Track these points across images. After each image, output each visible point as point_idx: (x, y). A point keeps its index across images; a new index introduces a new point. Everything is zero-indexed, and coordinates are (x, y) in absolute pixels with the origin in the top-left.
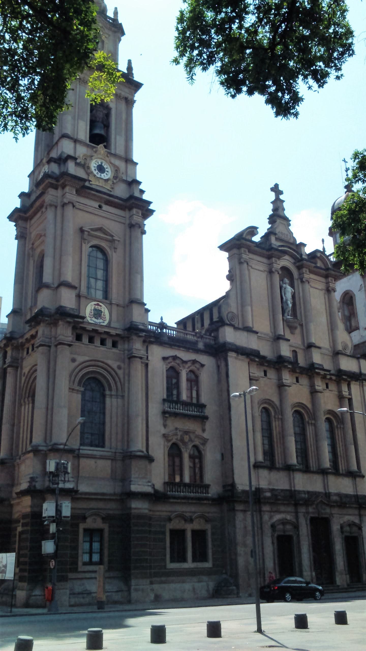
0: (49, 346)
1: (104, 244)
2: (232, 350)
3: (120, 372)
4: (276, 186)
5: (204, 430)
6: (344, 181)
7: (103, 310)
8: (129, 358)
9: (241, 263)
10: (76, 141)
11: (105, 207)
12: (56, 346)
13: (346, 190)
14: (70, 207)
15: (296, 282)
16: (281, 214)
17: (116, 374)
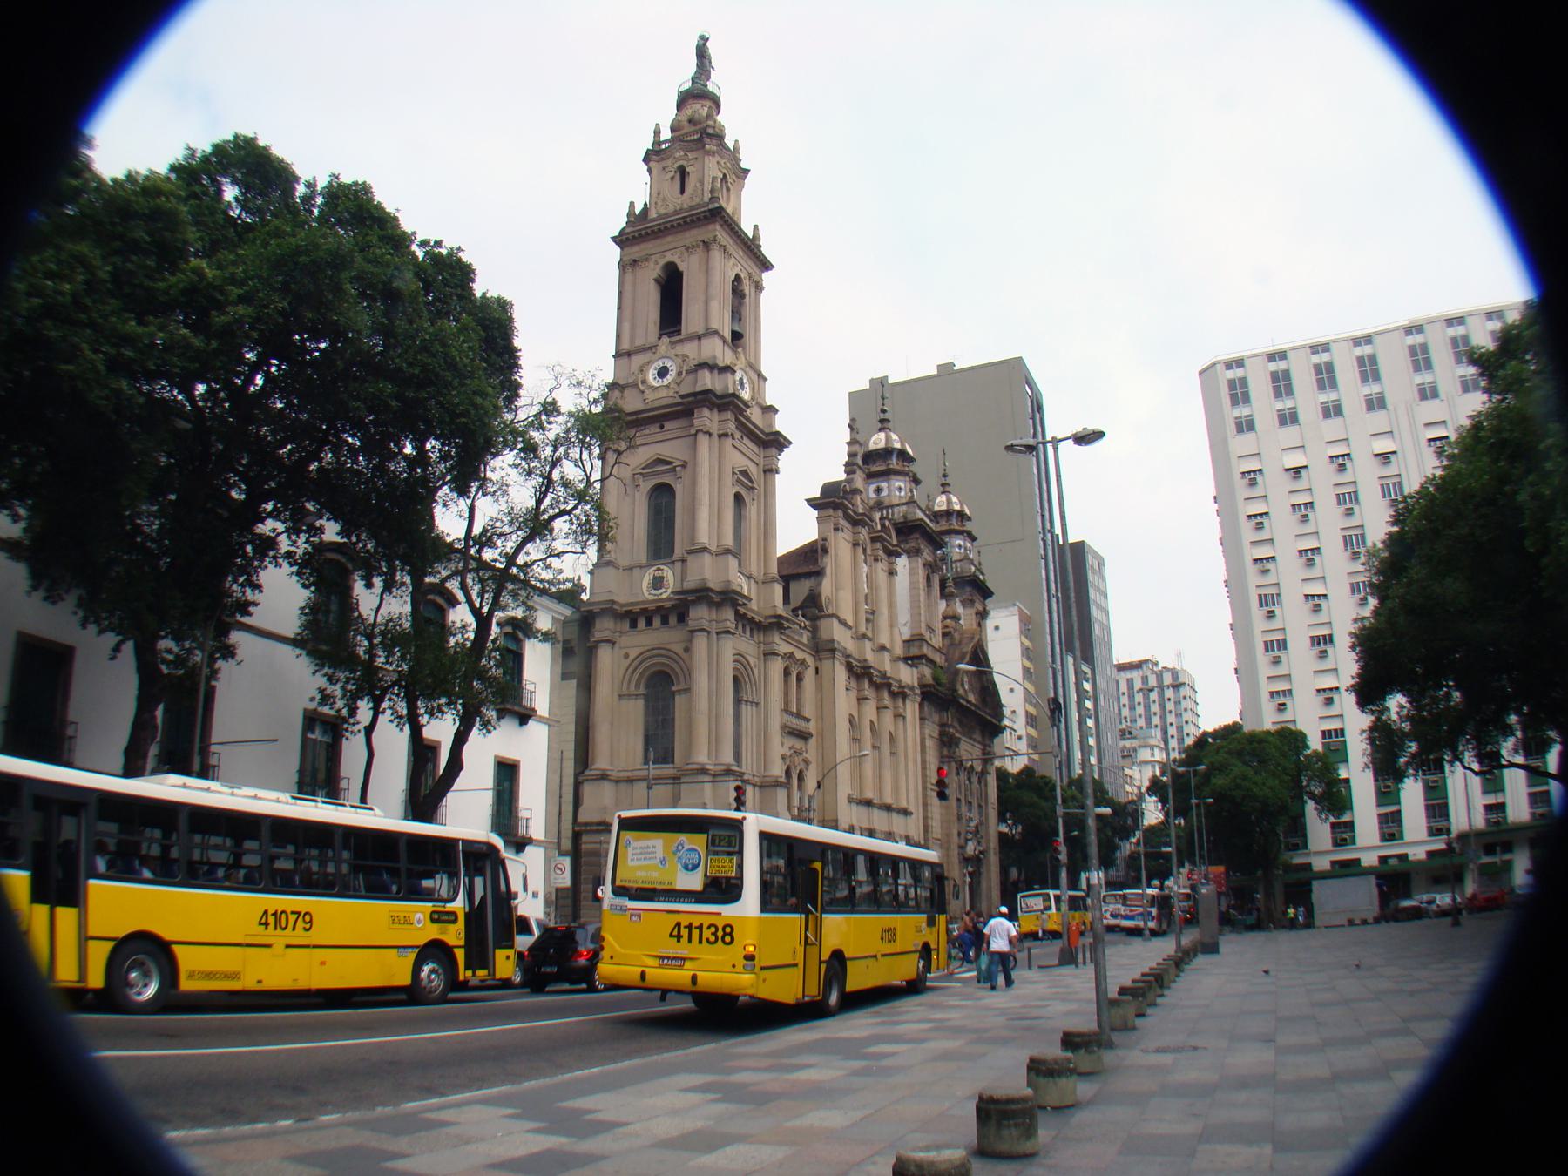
1: (743, 492)
8: (765, 655)
9: (836, 529)
11: (746, 441)
14: (729, 441)
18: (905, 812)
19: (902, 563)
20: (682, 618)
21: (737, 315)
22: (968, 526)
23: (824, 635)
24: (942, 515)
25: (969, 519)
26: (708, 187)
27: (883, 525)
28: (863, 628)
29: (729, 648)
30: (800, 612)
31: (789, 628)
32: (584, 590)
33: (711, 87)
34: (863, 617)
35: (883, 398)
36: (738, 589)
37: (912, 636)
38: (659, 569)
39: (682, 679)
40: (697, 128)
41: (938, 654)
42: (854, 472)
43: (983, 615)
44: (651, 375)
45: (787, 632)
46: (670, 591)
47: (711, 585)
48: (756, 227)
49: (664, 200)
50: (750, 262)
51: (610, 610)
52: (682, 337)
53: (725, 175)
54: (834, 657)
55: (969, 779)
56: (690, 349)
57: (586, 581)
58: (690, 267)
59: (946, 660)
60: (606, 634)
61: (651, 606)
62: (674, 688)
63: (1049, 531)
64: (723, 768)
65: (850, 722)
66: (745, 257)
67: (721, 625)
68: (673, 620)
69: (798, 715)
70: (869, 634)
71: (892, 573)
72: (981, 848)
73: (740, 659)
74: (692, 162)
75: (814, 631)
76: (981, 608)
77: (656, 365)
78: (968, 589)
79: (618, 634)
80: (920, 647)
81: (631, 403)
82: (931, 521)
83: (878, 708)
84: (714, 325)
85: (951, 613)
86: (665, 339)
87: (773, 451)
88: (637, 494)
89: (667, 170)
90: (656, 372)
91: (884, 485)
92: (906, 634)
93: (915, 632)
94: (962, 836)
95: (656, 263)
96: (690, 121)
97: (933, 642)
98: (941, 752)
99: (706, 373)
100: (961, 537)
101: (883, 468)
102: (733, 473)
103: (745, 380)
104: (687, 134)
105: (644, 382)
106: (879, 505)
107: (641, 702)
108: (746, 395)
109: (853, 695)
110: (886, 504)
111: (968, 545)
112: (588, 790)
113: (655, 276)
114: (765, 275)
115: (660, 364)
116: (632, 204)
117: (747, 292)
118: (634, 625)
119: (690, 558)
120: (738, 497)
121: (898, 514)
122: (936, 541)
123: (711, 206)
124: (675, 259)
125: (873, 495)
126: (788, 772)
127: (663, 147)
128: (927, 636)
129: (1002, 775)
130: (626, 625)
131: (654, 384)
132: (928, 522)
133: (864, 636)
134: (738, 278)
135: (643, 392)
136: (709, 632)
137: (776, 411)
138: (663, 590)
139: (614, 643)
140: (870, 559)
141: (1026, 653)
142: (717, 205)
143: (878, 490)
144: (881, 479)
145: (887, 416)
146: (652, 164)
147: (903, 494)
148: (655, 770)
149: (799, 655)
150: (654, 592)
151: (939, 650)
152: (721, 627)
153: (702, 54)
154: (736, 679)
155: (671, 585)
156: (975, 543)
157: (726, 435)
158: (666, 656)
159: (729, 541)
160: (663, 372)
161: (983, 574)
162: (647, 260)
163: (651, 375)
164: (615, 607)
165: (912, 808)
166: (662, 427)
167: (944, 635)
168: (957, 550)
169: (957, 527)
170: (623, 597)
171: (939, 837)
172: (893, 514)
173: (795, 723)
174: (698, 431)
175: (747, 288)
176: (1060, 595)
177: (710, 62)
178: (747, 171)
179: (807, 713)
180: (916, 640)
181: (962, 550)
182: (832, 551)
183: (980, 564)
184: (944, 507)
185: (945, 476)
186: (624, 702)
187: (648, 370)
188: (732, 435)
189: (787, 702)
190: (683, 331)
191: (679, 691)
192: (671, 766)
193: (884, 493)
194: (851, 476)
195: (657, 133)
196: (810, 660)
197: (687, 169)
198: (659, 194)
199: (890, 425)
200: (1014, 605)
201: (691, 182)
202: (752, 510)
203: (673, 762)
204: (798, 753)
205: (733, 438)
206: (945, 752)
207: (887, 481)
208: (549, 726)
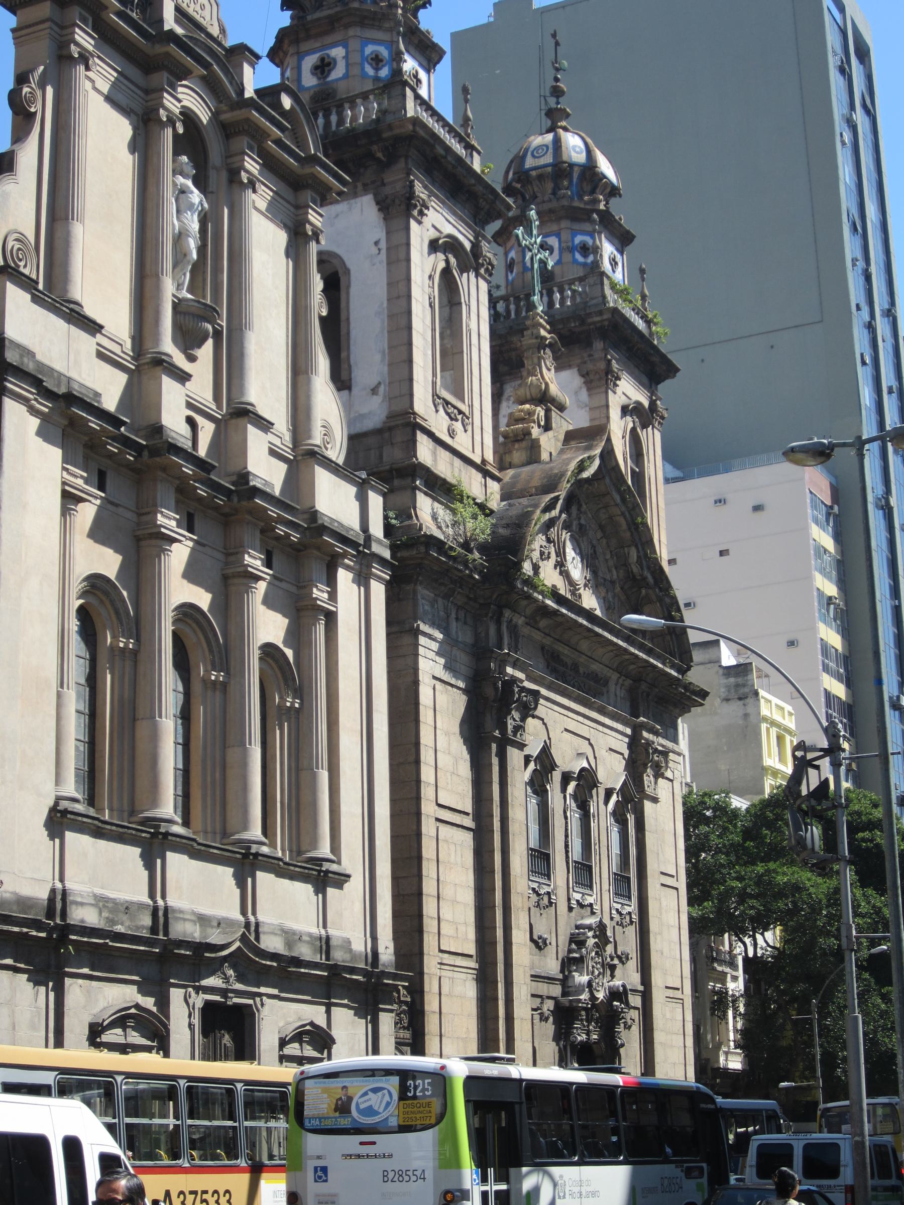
15: (212, 174)
25: (613, 192)
37: (391, 417)
41: (477, 477)
55: (583, 806)
70: (179, 359)
91: (338, 52)
97: (462, 443)
125: (309, 80)
128: (439, 423)
143: (323, 67)
144: (329, 39)
151: (482, 469)
161: (648, 322)
168: (579, 257)
185: (557, 92)
193: (338, 73)
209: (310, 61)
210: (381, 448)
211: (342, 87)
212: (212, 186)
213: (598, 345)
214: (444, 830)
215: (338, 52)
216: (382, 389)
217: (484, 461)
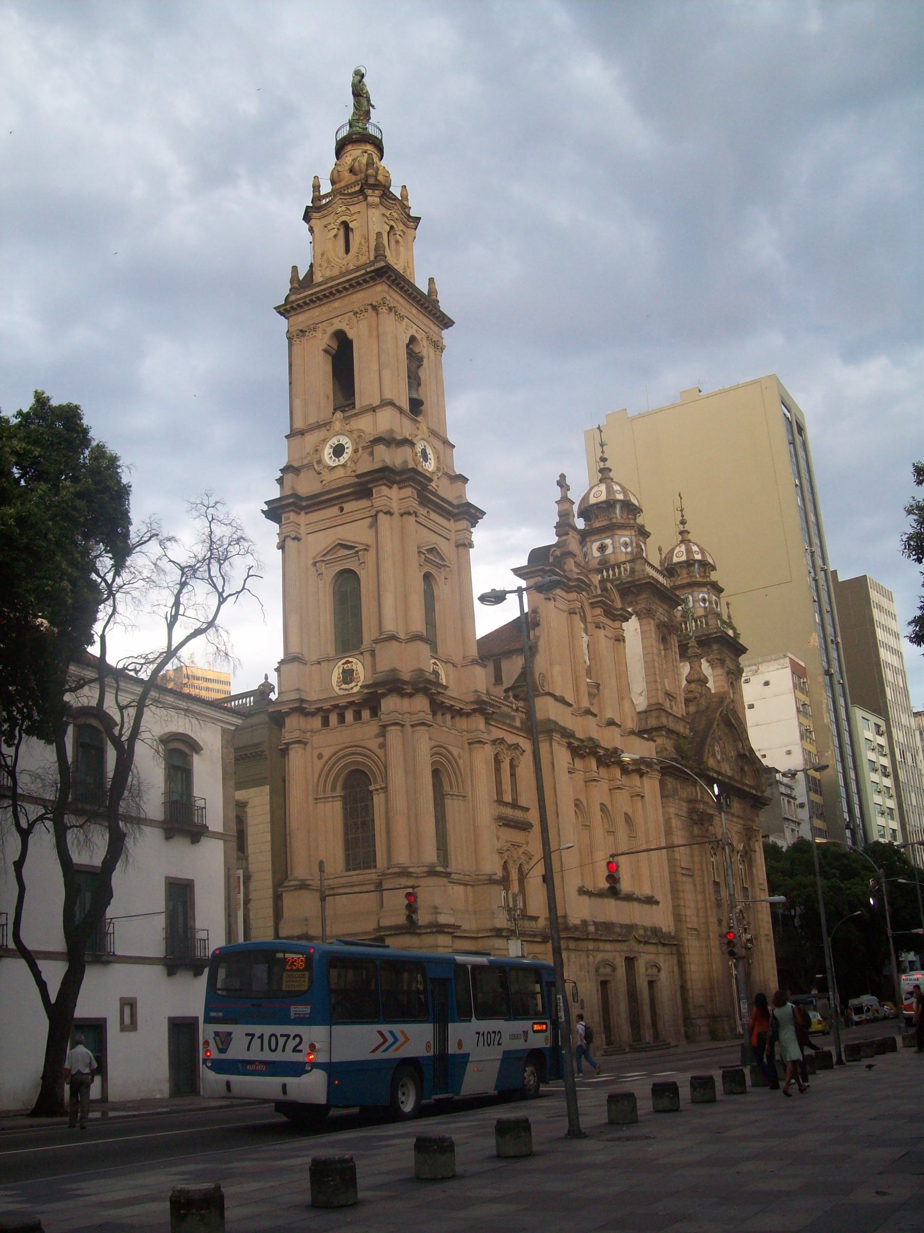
0: (403, 726)
1: (433, 571)
2: (557, 731)
3: (461, 762)
4: (563, 476)
5: (527, 843)
6: (598, 460)
7: (439, 671)
8: (470, 744)
10: (401, 410)
11: (434, 516)
12: (413, 726)
13: (600, 475)
15: (589, 625)
16: (572, 523)
17: (458, 765)
18: (650, 901)
19: (632, 627)
20: (375, 712)
21: (414, 380)
22: (714, 576)
23: (540, 715)
24: (681, 567)
26: (373, 243)
27: (604, 589)
28: (585, 704)
29: (424, 743)
30: (511, 694)
31: (494, 713)
32: (273, 690)
33: (372, 131)
34: (584, 691)
35: (602, 445)
36: (432, 678)
38: (348, 662)
39: (379, 779)
40: (359, 177)
41: (682, 723)
42: (567, 534)
43: (735, 675)
44: (327, 452)
45: (495, 716)
46: (360, 684)
47: (406, 677)
48: (431, 281)
49: (328, 261)
50: (426, 321)
51: (301, 709)
52: (356, 411)
53: (392, 227)
54: (551, 740)
56: (364, 424)
57: (274, 680)
58: (358, 332)
59: (691, 730)
60: (296, 735)
61: (342, 702)
62: (371, 788)
63: (822, 569)
64: (425, 869)
65: (576, 805)
66: (421, 317)
67: (415, 717)
68: (366, 714)
69: (515, 805)
70: (594, 709)
71: (620, 639)
72: (749, 936)
73: (440, 753)
74: (354, 217)
75: (530, 713)
76: (732, 667)
77: (330, 443)
78: (715, 647)
79: (308, 734)
80: (658, 717)
81: (307, 486)
82: (664, 576)
83: (610, 790)
84: (388, 395)
85: (696, 677)
86: (339, 415)
87: (463, 524)
88: (321, 584)
89: (330, 227)
90: (331, 450)
91: (608, 542)
92: (641, 703)
93: (654, 701)
94: (724, 923)
95: (325, 332)
96: (351, 170)
98: (691, 832)
99: (380, 449)
100: (705, 590)
101: (606, 523)
102: (419, 552)
103: (429, 451)
104: (348, 186)
105: (319, 462)
106: (604, 564)
107: (338, 805)
108: (430, 466)
109: (579, 777)
110: (612, 561)
111: (714, 598)
112: (288, 900)
113: (324, 346)
114: (445, 333)
115: (334, 441)
116: (295, 269)
117: (424, 353)
118: (326, 722)
119: (377, 647)
120: (427, 577)
121: (624, 573)
122: (670, 598)
123: (378, 266)
124: (343, 326)
125: (596, 554)
126: (505, 867)
127: (324, 202)
128: (667, 706)
129: (771, 851)
130: (317, 722)
131: (332, 464)
132: (660, 579)
133: (588, 712)
134: (413, 339)
135: (319, 473)
136: (403, 726)
137: (465, 480)
138: (353, 684)
139: (305, 744)
140: (591, 627)
141: (802, 710)
142: (383, 264)
143: (602, 548)
144: (604, 536)
145: (608, 464)
146: (313, 222)
147: (629, 549)
148: (356, 876)
149: (511, 739)
150: (344, 686)
152: (415, 719)
153: (359, 93)
154: (436, 773)
155: (362, 678)
156: (722, 595)
157: (409, 513)
158: (360, 754)
159: (418, 626)
160: (338, 451)
162: (315, 329)
163: (327, 454)
164: (305, 705)
165: (658, 897)
166: (342, 509)
167: (687, 701)
169: (699, 579)
170: (313, 694)
171: (696, 926)
172: (620, 573)
173: (509, 812)
174: (377, 512)
175: (424, 349)
176: (839, 640)
177: (369, 100)
178: (418, 219)
179: (523, 801)
180: (656, 709)
181: (707, 604)
182: (543, 623)
183: (729, 617)
184: (684, 558)
185: (683, 522)
186: (321, 806)
187: (323, 449)
188: (415, 513)
189: (499, 792)
190: (357, 406)
191: (377, 790)
192: (373, 871)
193: (609, 551)
194: (564, 538)
195: (316, 187)
196: (525, 744)
197: (351, 225)
198: (323, 255)
199: (611, 474)
200: (785, 656)
201: (356, 240)
202: (442, 590)
203: (375, 867)
204: (517, 846)
205: (416, 516)
206: (696, 830)
207: (611, 537)
208: (225, 841)
209: (596, 545)
210: (647, 718)
211: (612, 558)
212: (590, 632)
213: (715, 647)
214: (685, 878)
215: (608, 542)
216: (644, 694)
217: (683, 716)
